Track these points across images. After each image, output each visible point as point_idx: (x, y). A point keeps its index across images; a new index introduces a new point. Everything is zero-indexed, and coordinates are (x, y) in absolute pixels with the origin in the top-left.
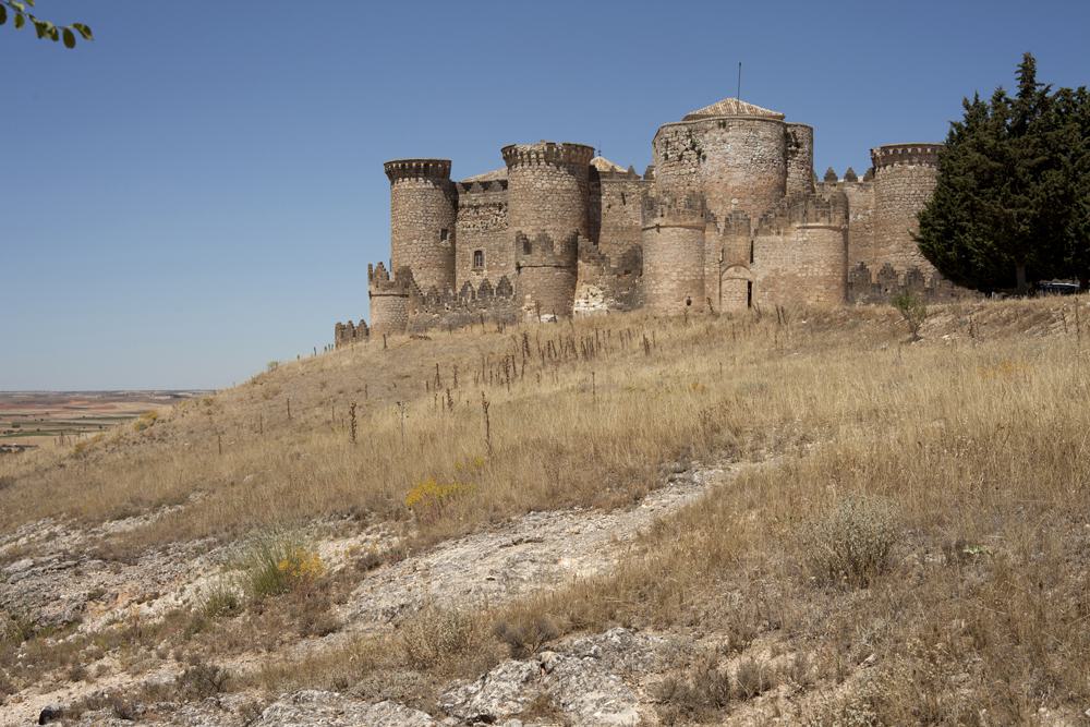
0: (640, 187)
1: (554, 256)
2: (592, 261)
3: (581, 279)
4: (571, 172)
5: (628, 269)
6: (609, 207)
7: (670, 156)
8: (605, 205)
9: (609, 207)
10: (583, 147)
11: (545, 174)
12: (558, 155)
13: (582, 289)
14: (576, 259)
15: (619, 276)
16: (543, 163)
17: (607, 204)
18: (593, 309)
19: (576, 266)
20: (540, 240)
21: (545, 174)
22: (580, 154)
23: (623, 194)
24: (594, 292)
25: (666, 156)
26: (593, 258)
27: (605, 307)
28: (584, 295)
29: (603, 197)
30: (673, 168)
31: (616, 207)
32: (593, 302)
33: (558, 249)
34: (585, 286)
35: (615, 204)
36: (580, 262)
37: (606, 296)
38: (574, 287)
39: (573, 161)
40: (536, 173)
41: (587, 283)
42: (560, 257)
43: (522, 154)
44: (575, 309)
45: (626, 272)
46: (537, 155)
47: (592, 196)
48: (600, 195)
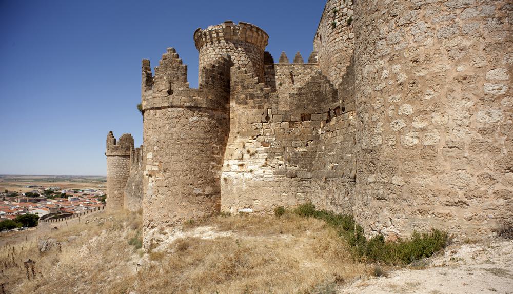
0: (305, 68)
1: (188, 91)
2: (251, 101)
3: (234, 129)
4: (247, 51)
5: (307, 112)
6: (281, 84)
7: (338, 23)
8: (278, 83)
9: (281, 84)
10: (258, 29)
11: (224, 50)
12: (235, 34)
13: (235, 145)
14: (227, 100)
15: (292, 123)
16: (222, 41)
17: (279, 82)
18: (249, 176)
19: (227, 110)
20: (166, 66)
21: (224, 50)
22: (255, 34)
23: (291, 74)
24: (252, 147)
25: (334, 25)
26: (252, 97)
27: (269, 171)
28: (237, 154)
29: (276, 77)
30: (341, 34)
31: (286, 85)
32: (250, 163)
33: (197, 80)
34: (239, 140)
35: (285, 82)
36: (233, 104)
37: (271, 155)
38: (223, 142)
39: (249, 40)
40: (217, 50)
41: (242, 135)
42: (198, 92)
43: (205, 34)
44: (224, 175)
45: (303, 118)
46: (218, 34)
47: (267, 76)
48: (274, 75)
